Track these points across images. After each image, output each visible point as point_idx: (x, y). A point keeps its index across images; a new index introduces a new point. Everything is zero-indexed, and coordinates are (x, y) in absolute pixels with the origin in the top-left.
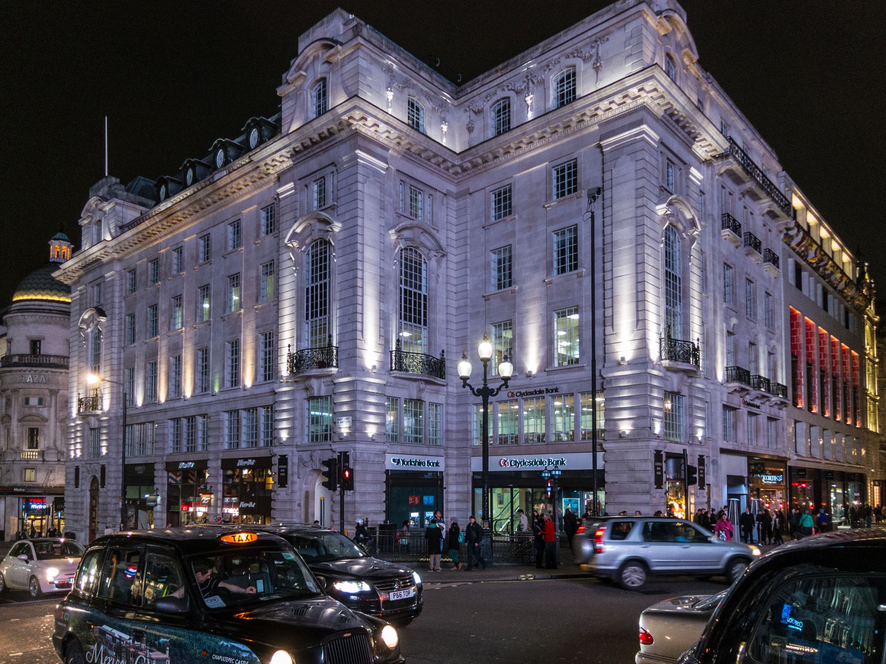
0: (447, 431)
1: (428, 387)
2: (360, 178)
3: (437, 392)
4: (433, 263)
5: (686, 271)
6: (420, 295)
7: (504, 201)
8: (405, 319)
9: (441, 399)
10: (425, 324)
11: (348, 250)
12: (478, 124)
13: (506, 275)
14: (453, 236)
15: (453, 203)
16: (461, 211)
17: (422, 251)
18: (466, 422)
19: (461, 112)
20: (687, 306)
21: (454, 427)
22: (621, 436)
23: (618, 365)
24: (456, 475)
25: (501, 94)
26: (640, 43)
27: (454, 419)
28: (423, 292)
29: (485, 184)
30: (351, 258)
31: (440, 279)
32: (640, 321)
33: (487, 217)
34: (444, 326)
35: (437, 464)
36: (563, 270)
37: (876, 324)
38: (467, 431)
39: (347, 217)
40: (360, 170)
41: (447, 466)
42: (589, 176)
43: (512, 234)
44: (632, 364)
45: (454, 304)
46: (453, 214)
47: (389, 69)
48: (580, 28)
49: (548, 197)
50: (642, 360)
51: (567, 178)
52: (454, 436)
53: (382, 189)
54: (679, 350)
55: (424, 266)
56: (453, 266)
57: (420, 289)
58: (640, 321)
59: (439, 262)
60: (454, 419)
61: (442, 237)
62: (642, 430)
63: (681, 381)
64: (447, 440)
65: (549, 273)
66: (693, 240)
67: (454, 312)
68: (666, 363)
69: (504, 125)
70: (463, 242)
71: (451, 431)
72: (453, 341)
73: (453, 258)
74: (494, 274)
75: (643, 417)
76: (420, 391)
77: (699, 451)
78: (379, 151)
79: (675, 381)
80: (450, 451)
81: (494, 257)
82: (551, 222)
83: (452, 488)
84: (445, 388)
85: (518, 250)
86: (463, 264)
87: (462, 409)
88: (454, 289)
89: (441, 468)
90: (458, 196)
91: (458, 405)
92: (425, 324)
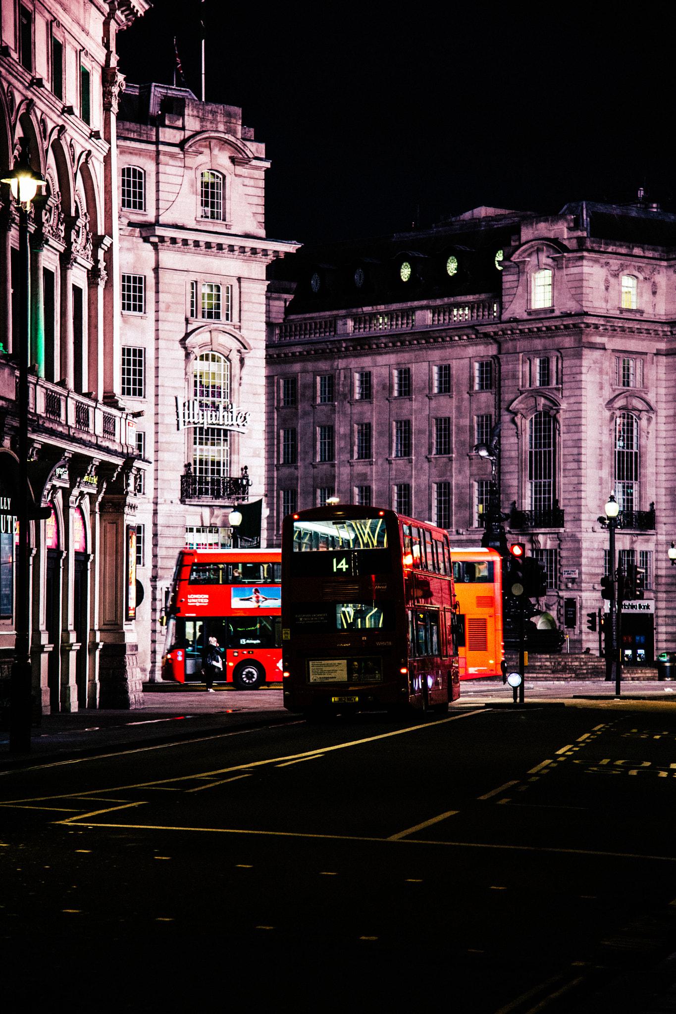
0: (657, 576)
1: (640, 537)
2: (584, 370)
3: (647, 541)
4: (644, 422)
6: (631, 453)
8: (619, 479)
9: (651, 547)
10: (636, 480)
11: (574, 429)
24: (665, 616)
28: (635, 450)
31: (650, 436)
34: (654, 478)
35: (648, 607)
41: (657, 608)
52: (663, 580)
55: (635, 424)
57: (632, 448)
59: (649, 419)
61: (651, 397)
64: (657, 584)
67: (663, 463)
71: (661, 576)
80: (660, 595)
83: (662, 629)
84: (654, 537)
88: (663, 442)
89: (652, 610)
92: (636, 480)
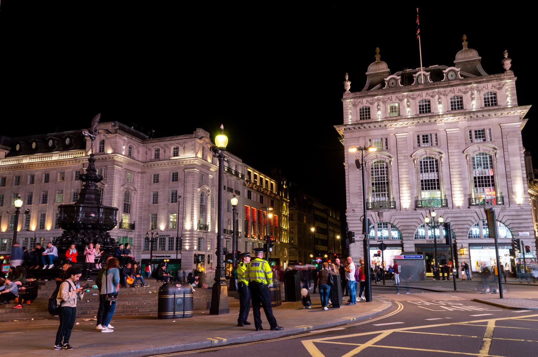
5: (206, 203)
7: (156, 179)
12: (149, 153)
13: (156, 200)
14: (139, 185)
15: (140, 175)
16: (142, 178)
17: (130, 191)
18: (141, 243)
19: (144, 148)
20: (206, 213)
21: (136, 245)
22: (186, 250)
23: (186, 231)
25: (157, 147)
26: (195, 147)
27: (136, 242)
29: (151, 172)
30: (110, 196)
32: (192, 219)
33: (151, 182)
36: (173, 202)
37: (289, 202)
38: (140, 246)
39: (110, 183)
40: (115, 171)
42: (181, 176)
43: (158, 188)
44: (189, 231)
45: (138, 206)
46: (139, 178)
47: (124, 140)
48: (180, 137)
49: (169, 180)
50: (192, 230)
51: (175, 177)
53: (120, 175)
54: (203, 227)
56: (139, 194)
58: (192, 219)
60: (136, 242)
61: (136, 186)
62: (191, 249)
63: (203, 235)
65: (169, 202)
66: (209, 195)
67: (138, 208)
68: (198, 230)
69: (157, 156)
70: (142, 188)
72: (137, 218)
73: (139, 192)
74: (152, 198)
75: (192, 245)
76: (127, 234)
77: (208, 253)
78: (120, 164)
79: (201, 235)
81: (152, 193)
82: (170, 188)
85: (160, 193)
86: (142, 194)
87: (139, 239)
90: (142, 173)
91: (138, 238)
